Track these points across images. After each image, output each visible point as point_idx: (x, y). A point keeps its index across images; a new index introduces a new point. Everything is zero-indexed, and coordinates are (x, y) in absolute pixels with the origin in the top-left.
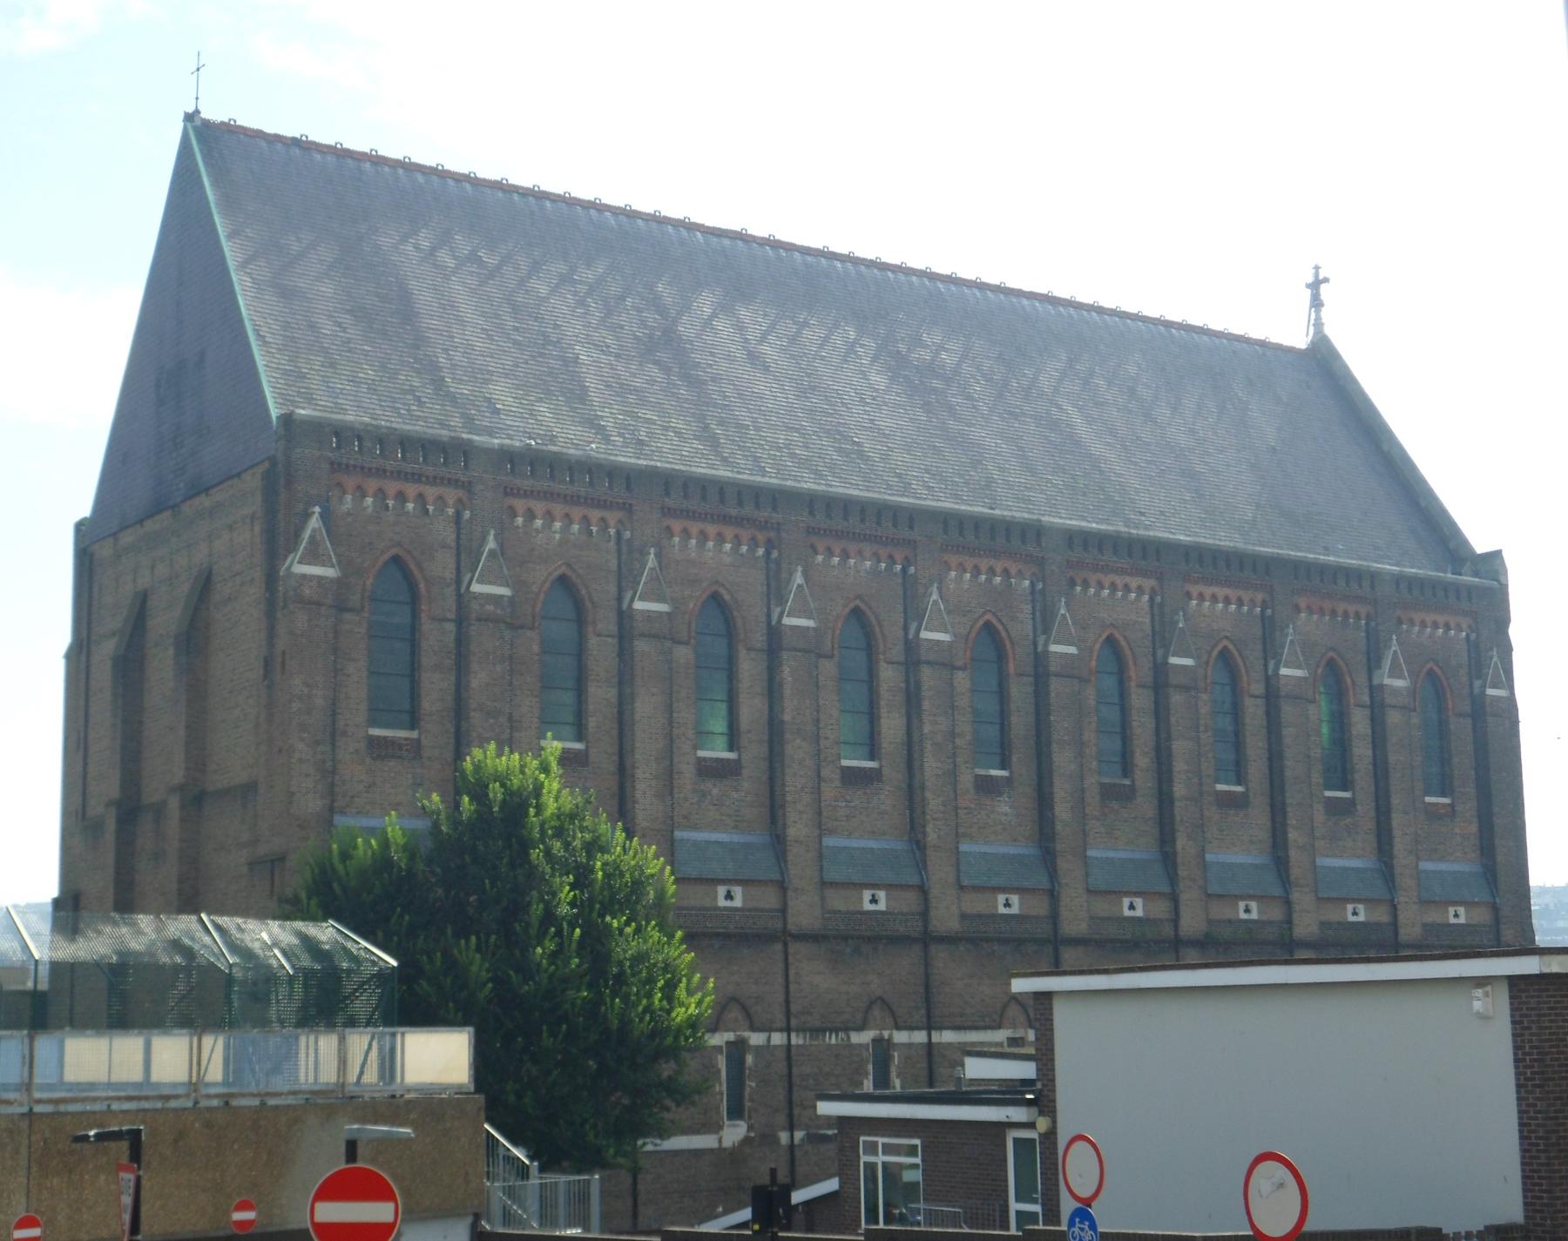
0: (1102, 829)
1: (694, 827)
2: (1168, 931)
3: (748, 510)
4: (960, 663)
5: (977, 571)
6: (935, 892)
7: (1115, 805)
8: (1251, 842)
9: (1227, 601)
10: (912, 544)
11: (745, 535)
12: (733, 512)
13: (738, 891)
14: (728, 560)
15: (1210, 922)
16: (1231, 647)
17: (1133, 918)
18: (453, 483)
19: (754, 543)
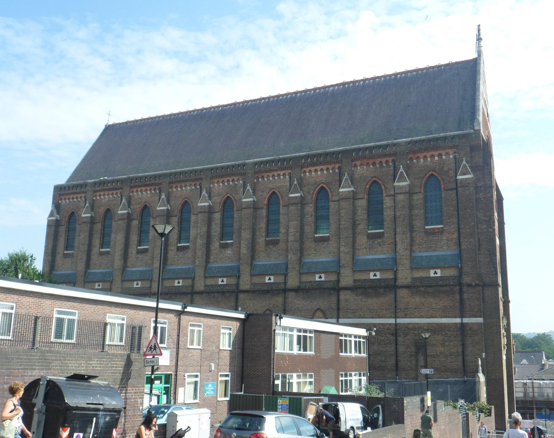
0: (265, 255)
1: (134, 267)
2: (282, 286)
4: (217, 211)
5: (223, 182)
6: (197, 279)
7: (271, 246)
8: (330, 253)
9: (322, 170)
10: (201, 179)
11: (153, 188)
12: (149, 183)
13: (140, 283)
14: (149, 195)
15: (300, 282)
16: (324, 186)
17: (270, 283)
18: (83, 192)
19: (155, 189)
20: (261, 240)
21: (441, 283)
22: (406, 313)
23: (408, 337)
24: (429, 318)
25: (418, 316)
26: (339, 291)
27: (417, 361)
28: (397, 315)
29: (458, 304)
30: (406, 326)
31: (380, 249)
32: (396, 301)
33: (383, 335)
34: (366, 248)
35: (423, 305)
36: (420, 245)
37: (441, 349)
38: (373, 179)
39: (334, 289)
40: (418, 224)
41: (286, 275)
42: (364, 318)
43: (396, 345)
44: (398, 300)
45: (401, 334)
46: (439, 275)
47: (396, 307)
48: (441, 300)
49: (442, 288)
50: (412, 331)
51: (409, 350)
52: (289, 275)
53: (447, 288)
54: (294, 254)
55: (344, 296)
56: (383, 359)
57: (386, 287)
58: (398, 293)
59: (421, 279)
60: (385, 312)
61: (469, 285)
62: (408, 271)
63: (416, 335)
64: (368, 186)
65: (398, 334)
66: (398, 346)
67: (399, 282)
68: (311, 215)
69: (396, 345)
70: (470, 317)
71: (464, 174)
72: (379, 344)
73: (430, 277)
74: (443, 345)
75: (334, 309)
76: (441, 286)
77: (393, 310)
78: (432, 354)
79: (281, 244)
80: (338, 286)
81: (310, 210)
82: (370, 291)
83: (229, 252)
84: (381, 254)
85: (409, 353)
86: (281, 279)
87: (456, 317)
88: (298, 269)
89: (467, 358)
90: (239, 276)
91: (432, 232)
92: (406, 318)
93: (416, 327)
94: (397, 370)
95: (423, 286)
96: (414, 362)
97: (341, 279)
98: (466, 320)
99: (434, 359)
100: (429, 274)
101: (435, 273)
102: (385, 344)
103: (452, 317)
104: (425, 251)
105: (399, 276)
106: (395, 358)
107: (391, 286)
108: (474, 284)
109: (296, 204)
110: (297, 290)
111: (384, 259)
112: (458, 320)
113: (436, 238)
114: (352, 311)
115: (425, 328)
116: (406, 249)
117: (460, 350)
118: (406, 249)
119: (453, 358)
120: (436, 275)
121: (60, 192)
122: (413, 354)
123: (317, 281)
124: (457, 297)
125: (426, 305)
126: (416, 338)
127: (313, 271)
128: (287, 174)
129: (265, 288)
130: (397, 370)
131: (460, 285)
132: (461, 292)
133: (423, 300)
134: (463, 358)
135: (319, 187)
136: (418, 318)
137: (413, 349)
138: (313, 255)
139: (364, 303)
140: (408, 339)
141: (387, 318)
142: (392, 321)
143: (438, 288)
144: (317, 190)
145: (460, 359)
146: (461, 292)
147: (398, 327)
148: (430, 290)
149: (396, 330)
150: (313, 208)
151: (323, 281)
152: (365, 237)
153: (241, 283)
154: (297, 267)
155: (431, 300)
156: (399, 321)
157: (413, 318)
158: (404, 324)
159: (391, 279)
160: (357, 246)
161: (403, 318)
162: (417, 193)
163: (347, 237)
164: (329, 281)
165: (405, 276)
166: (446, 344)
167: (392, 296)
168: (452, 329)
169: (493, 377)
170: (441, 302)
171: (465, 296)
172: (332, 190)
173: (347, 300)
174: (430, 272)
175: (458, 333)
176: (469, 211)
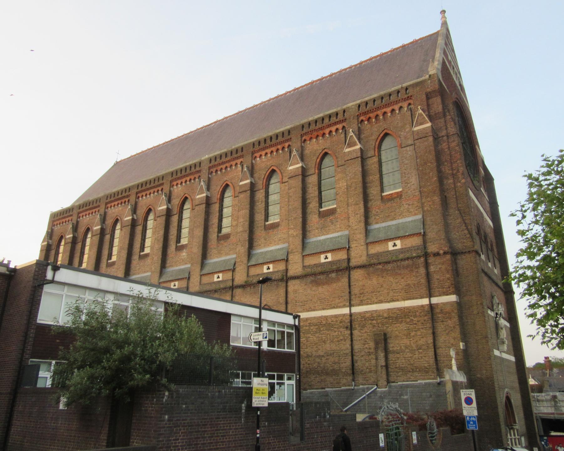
2: (230, 284)
3: (124, 194)
7: (222, 242)
8: (280, 240)
14: (120, 209)
16: (275, 168)
20: (213, 235)
21: (401, 256)
22: (361, 298)
23: (365, 329)
24: (389, 302)
25: (376, 300)
26: (287, 282)
27: (377, 359)
28: (352, 302)
29: (423, 281)
30: (362, 315)
31: (332, 227)
32: (350, 286)
33: (336, 330)
34: (317, 229)
35: (382, 286)
36: (377, 215)
37: (406, 341)
38: (324, 152)
39: (281, 280)
40: (373, 192)
41: (234, 270)
42: (314, 310)
43: (352, 341)
44: (352, 284)
45: (357, 326)
46: (399, 246)
47: (350, 292)
48: (402, 278)
49: (403, 263)
50: (370, 322)
51: (366, 346)
52: (237, 269)
53: (410, 262)
54: (242, 246)
55: (293, 285)
56: (336, 359)
57: (338, 270)
58: (351, 276)
59: (378, 255)
60: (337, 301)
61: (437, 254)
62: (363, 247)
63: (374, 326)
64: (318, 160)
65: (353, 326)
66: (354, 342)
67: (353, 263)
68: (262, 202)
69: (352, 341)
70: (440, 296)
71: (421, 124)
72: (332, 342)
73: (388, 251)
74: (408, 335)
75: (281, 304)
76: (402, 260)
77: (347, 297)
78: (395, 349)
79: (232, 237)
80: (286, 276)
81: (261, 197)
82: (322, 277)
83: (184, 254)
84: (334, 234)
85: (367, 351)
86: (229, 275)
87: (422, 298)
88: (246, 262)
89: (439, 351)
90: (189, 278)
91: (391, 198)
92: (362, 305)
93: (375, 315)
94: (353, 373)
95: (380, 264)
96: (373, 362)
97: (290, 267)
98: (435, 300)
99: (398, 355)
100: (388, 248)
101: (395, 245)
102: (338, 341)
103: (417, 298)
104: (383, 222)
105: (353, 254)
106: (350, 358)
107: (345, 269)
108: (441, 252)
109: (245, 191)
110: (243, 286)
111: (336, 237)
112: (425, 301)
113: (395, 204)
114: (301, 304)
115: (385, 315)
116: (360, 221)
117: (430, 340)
118: (360, 221)
119: (421, 353)
120: (395, 248)
121: (58, 218)
122: (372, 350)
123: (265, 273)
124: (422, 271)
125: (384, 286)
126: (375, 329)
127: (261, 261)
128: (239, 163)
129: (214, 287)
130: (353, 373)
131: (426, 255)
132: (427, 265)
133: (381, 280)
134: (435, 351)
135: (270, 171)
136: (376, 303)
137: (372, 345)
138: (262, 245)
139: (314, 292)
140: (366, 332)
141: (340, 307)
142: (346, 311)
143: (399, 264)
144: (267, 174)
145: (431, 353)
146: (427, 265)
147: (353, 318)
148: (389, 266)
149: (351, 322)
150: (264, 194)
151: (270, 272)
152: (317, 216)
153: (191, 285)
154: (245, 259)
155: (392, 279)
156: (355, 310)
157: (371, 304)
158: (360, 314)
159: (344, 260)
160: (308, 228)
161: (359, 305)
162: (371, 157)
163: (295, 218)
164: (277, 271)
165: (359, 255)
166: (412, 334)
167: (345, 280)
168: (417, 314)
169: (479, 376)
170: (403, 280)
171: (432, 269)
172: (282, 171)
173: (295, 291)
174: (388, 245)
175: (426, 318)
176: (429, 164)
